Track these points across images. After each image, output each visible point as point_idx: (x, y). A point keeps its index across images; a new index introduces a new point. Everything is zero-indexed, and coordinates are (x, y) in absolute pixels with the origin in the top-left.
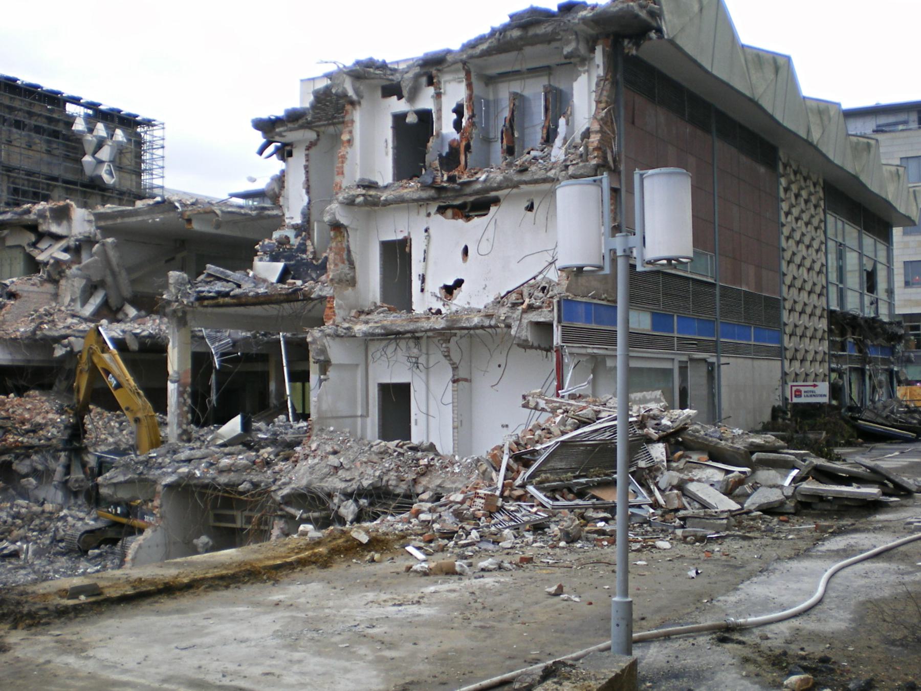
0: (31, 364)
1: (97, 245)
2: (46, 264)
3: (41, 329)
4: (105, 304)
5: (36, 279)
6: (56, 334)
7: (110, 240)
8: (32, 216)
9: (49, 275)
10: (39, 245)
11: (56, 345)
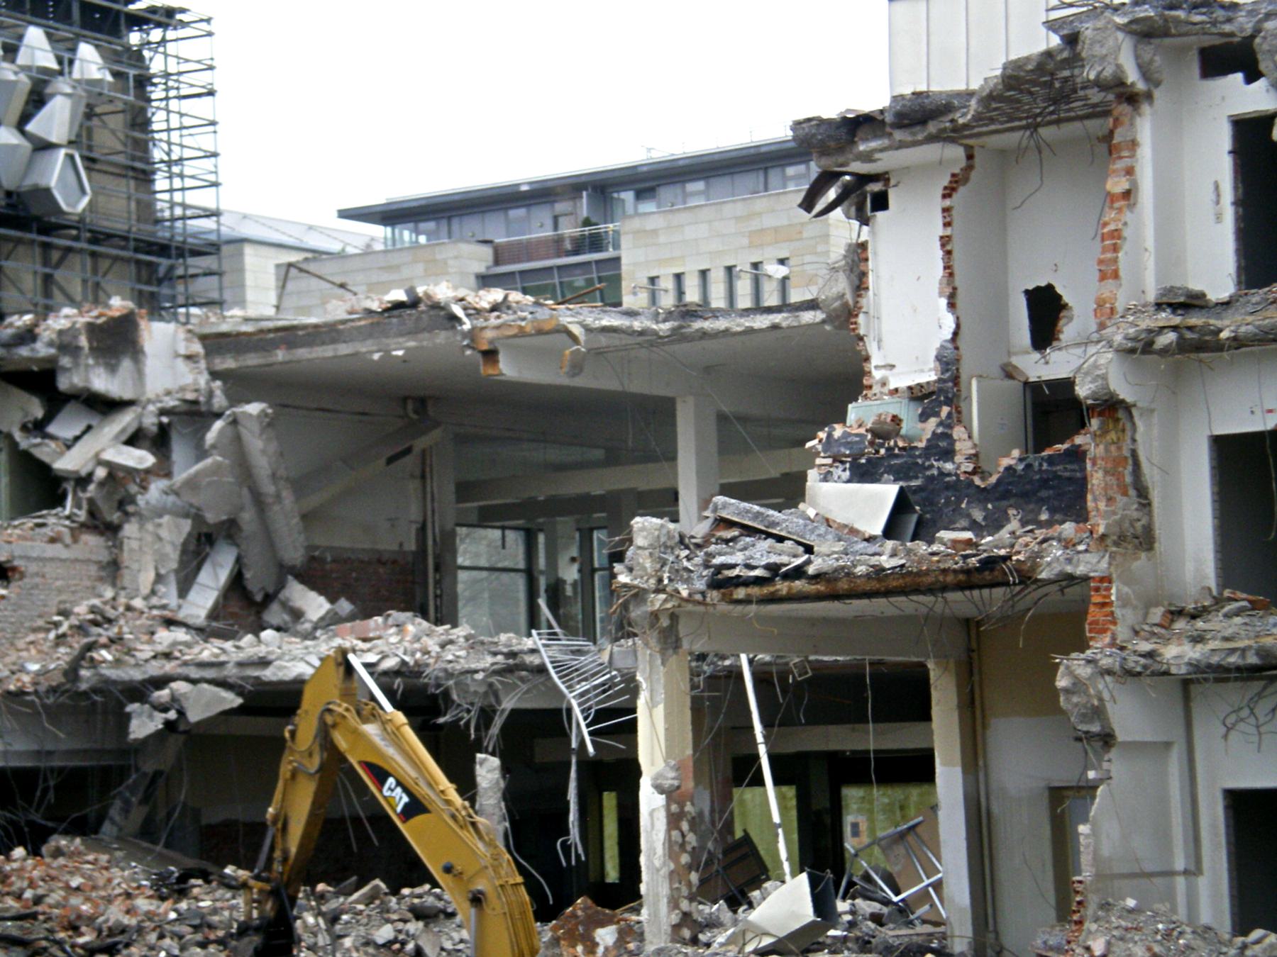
0: (57, 763)
1: (218, 425)
2: (83, 481)
3: (94, 664)
4: (237, 583)
5: (56, 520)
6: (137, 675)
7: (254, 408)
8: (42, 349)
9: (92, 513)
10: (52, 429)
11: (132, 707)
